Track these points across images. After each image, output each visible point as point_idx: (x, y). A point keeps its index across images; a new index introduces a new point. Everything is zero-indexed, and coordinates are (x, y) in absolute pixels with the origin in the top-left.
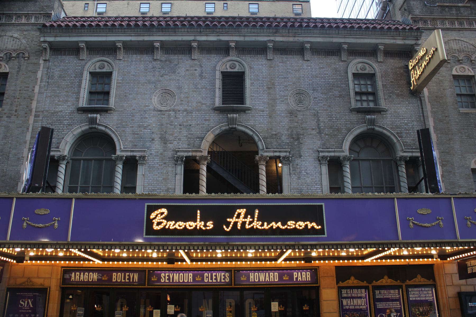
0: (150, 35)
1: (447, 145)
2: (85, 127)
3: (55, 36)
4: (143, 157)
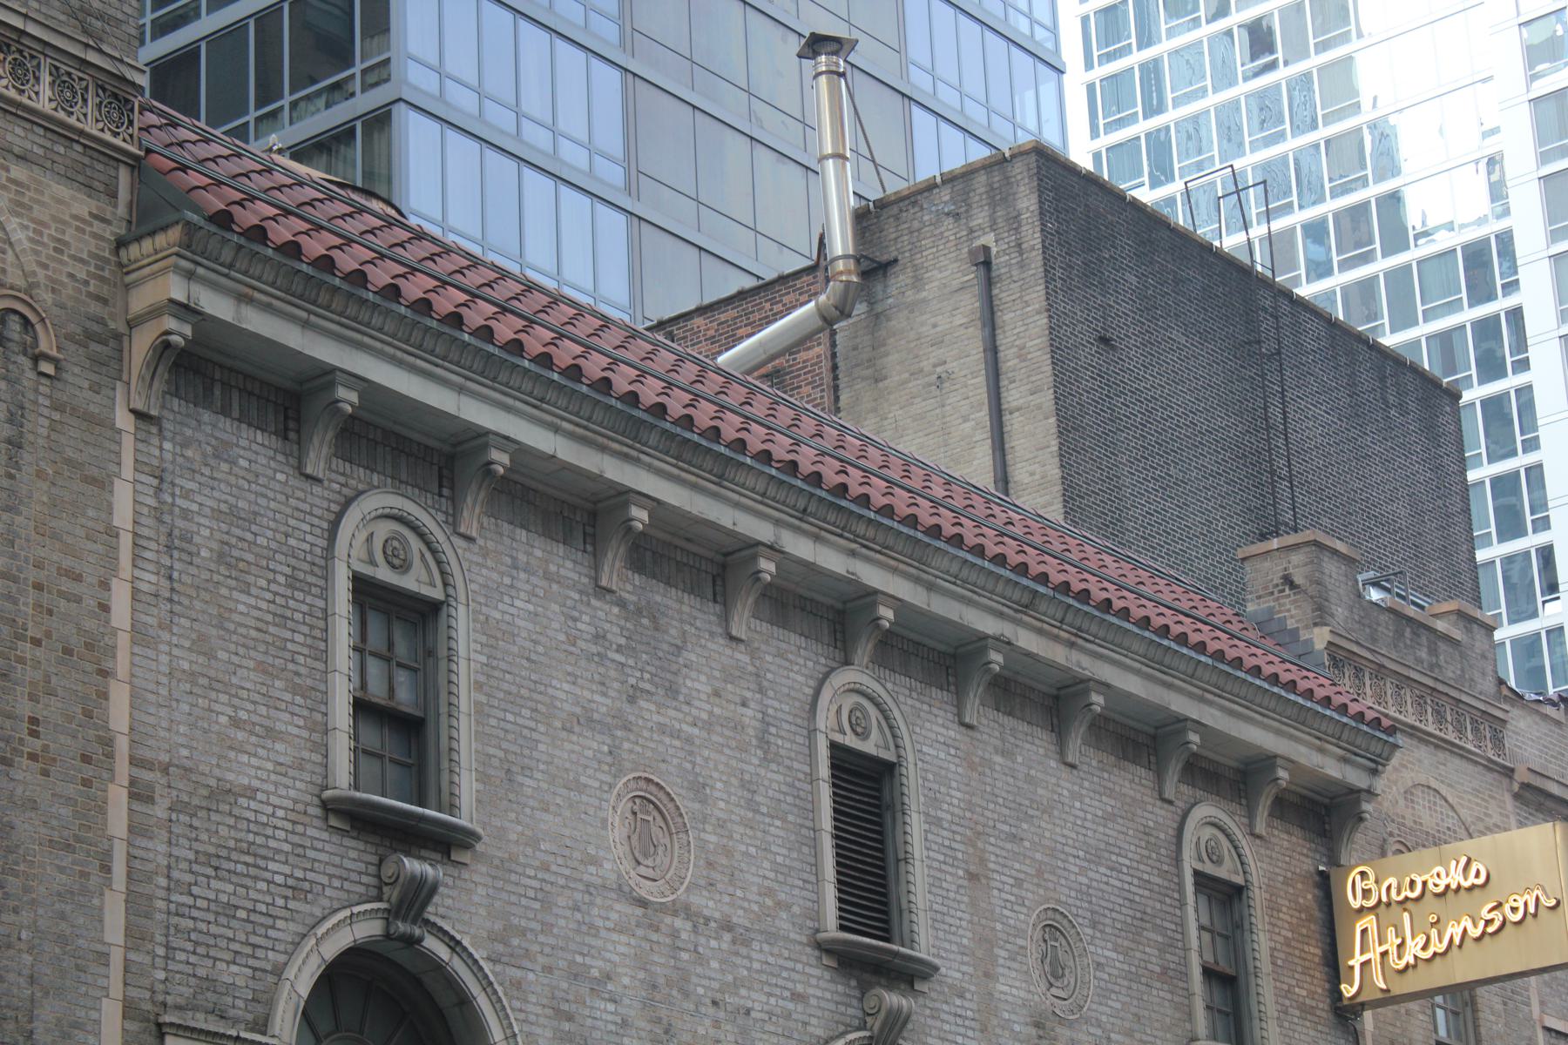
0: (626, 457)
2: (368, 930)
3: (242, 299)
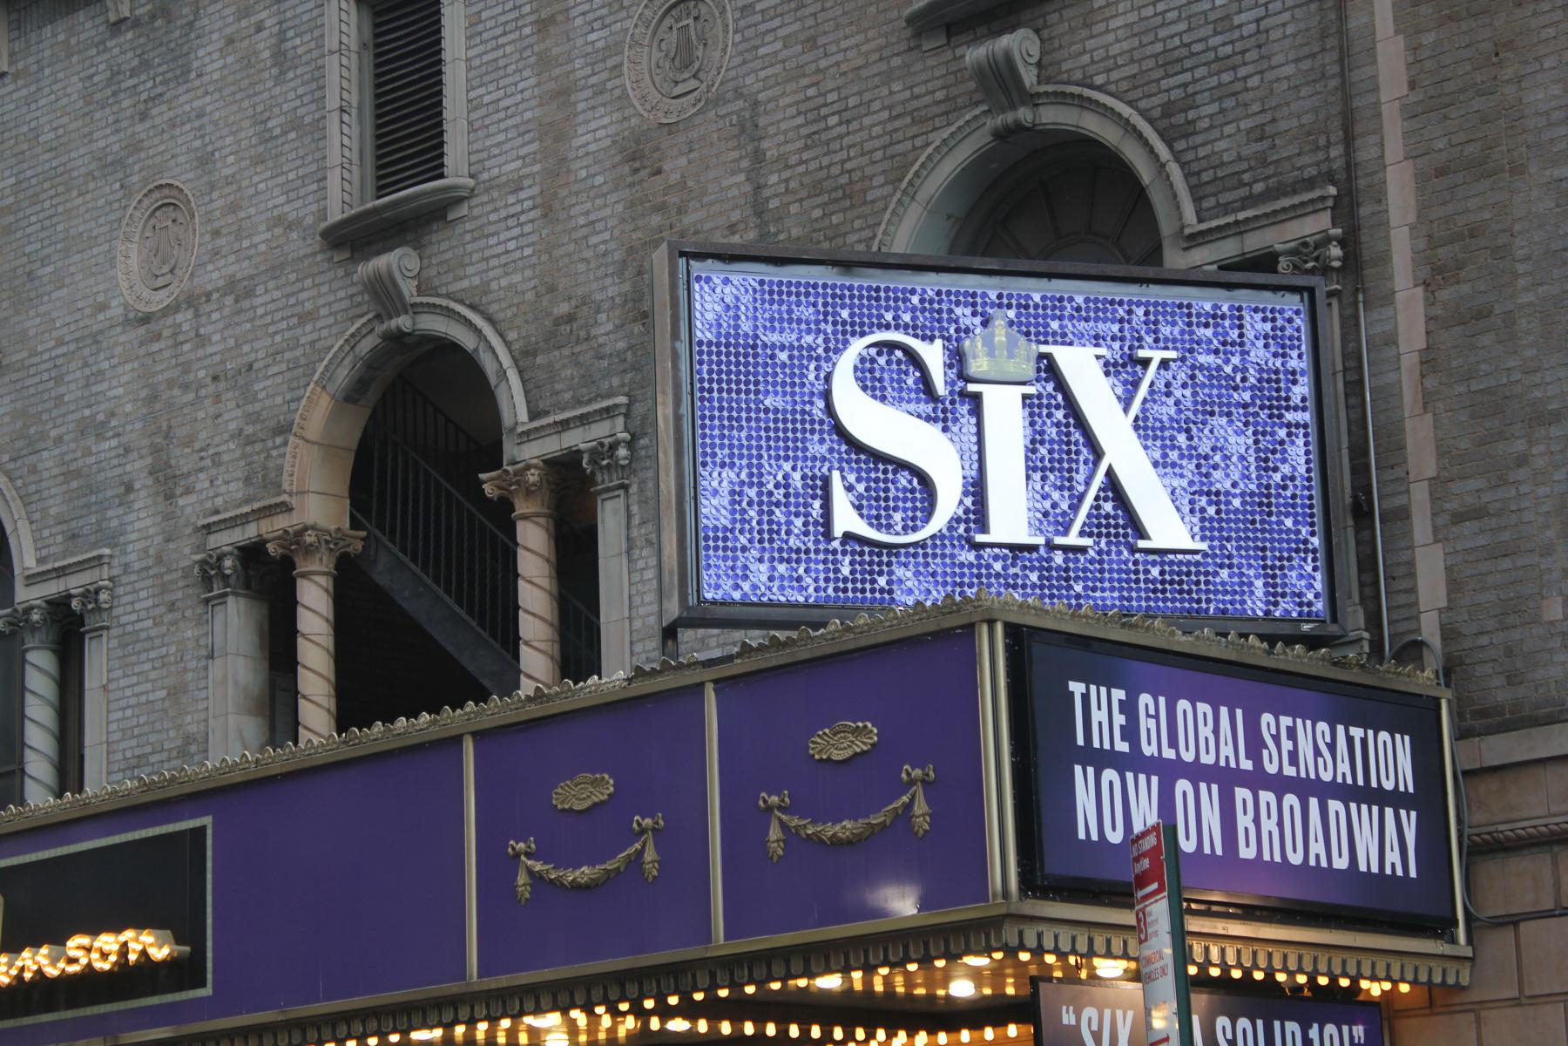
1: (1477, 104)
4: (91, 594)
